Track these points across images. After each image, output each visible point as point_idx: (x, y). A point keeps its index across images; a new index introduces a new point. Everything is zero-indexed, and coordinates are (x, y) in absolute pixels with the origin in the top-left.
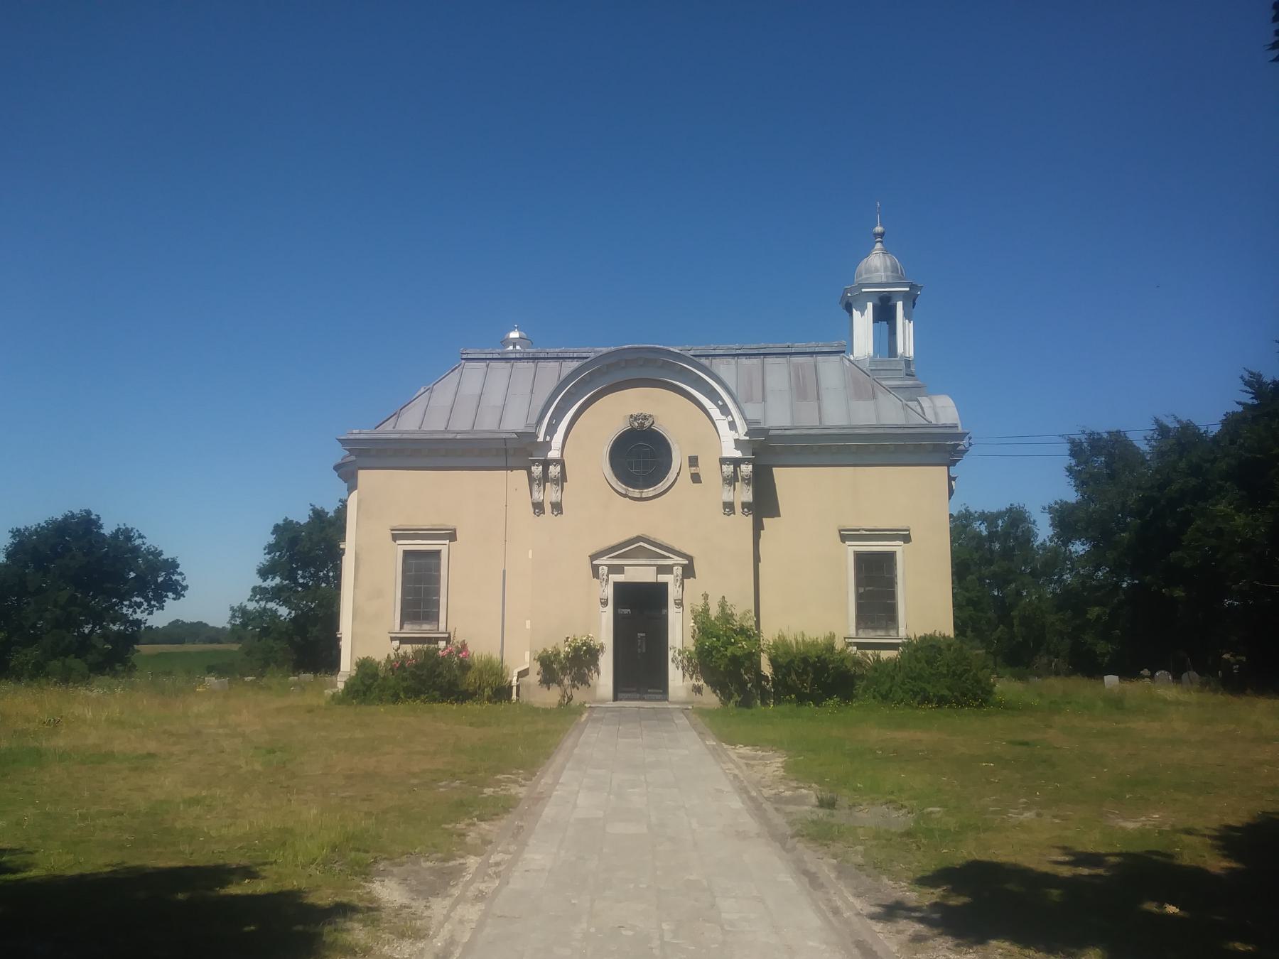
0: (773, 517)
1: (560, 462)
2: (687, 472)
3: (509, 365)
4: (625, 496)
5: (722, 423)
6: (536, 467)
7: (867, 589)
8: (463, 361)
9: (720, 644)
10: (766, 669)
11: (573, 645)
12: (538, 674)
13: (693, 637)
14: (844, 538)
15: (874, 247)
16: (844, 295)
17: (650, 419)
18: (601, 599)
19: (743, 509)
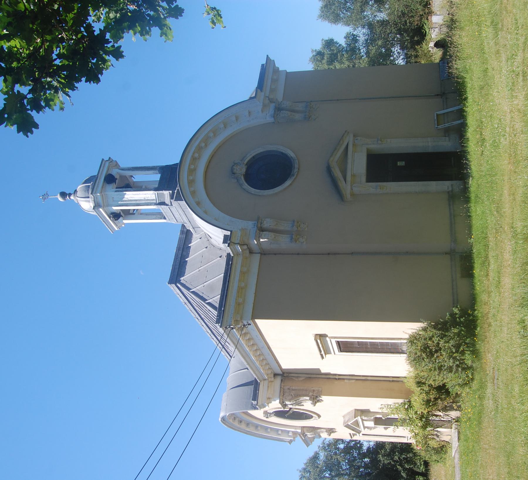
0: (320, 371)
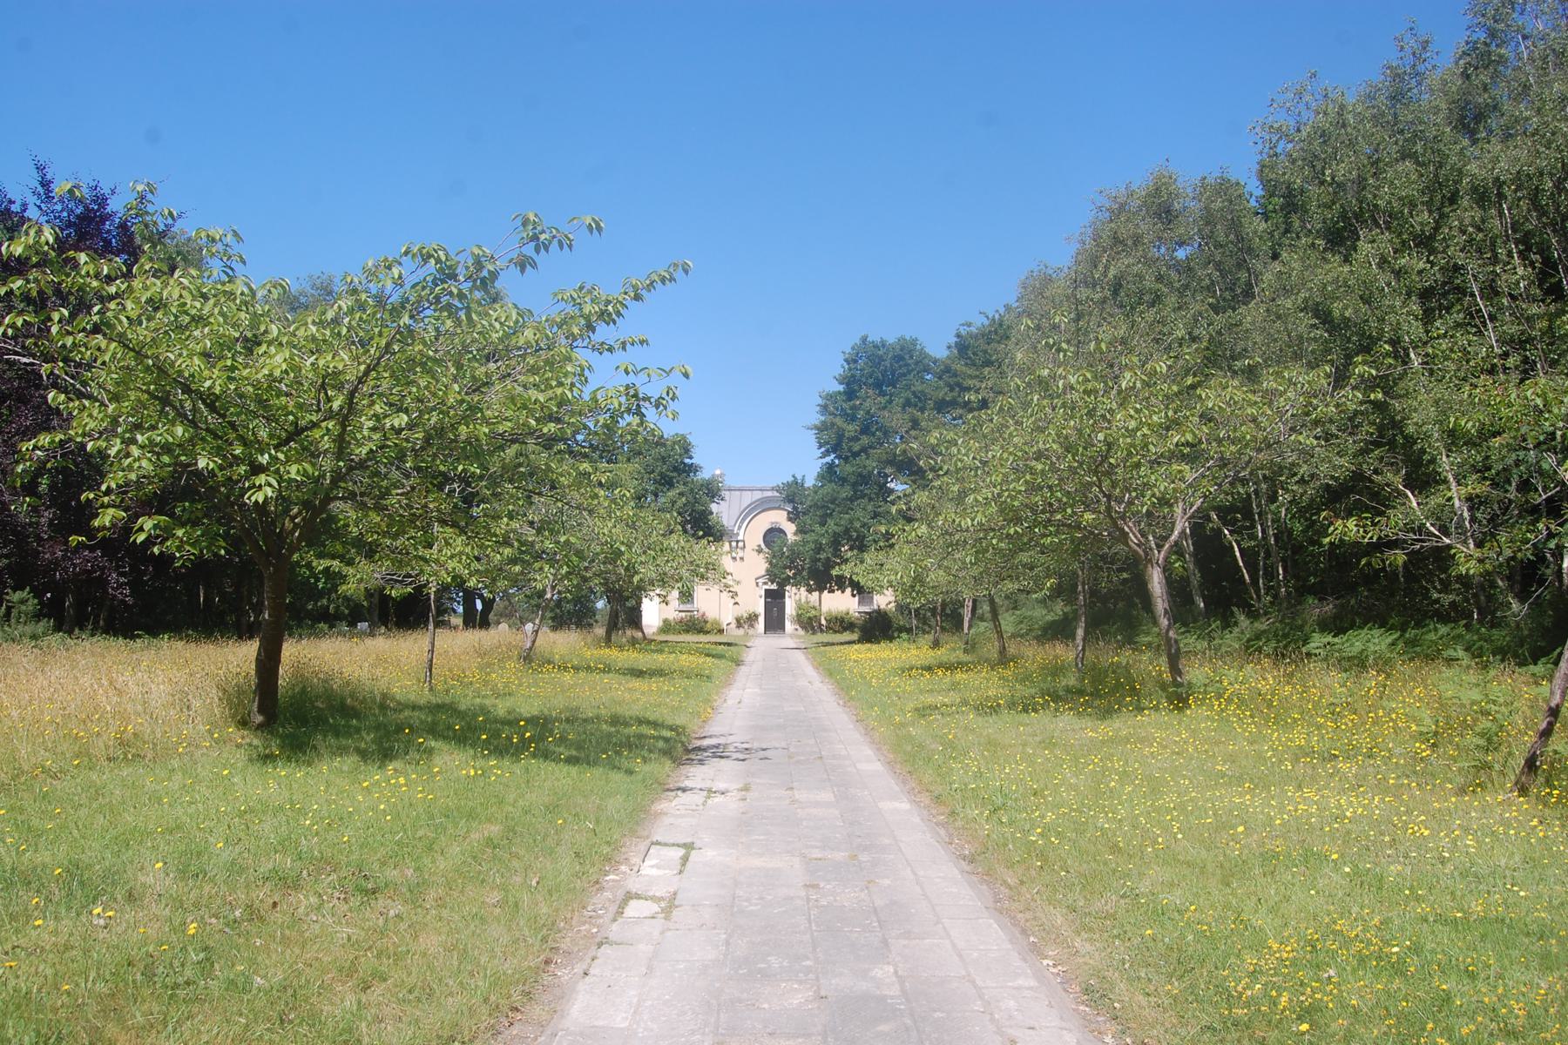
1: (744, 541)
10: (823, 622)
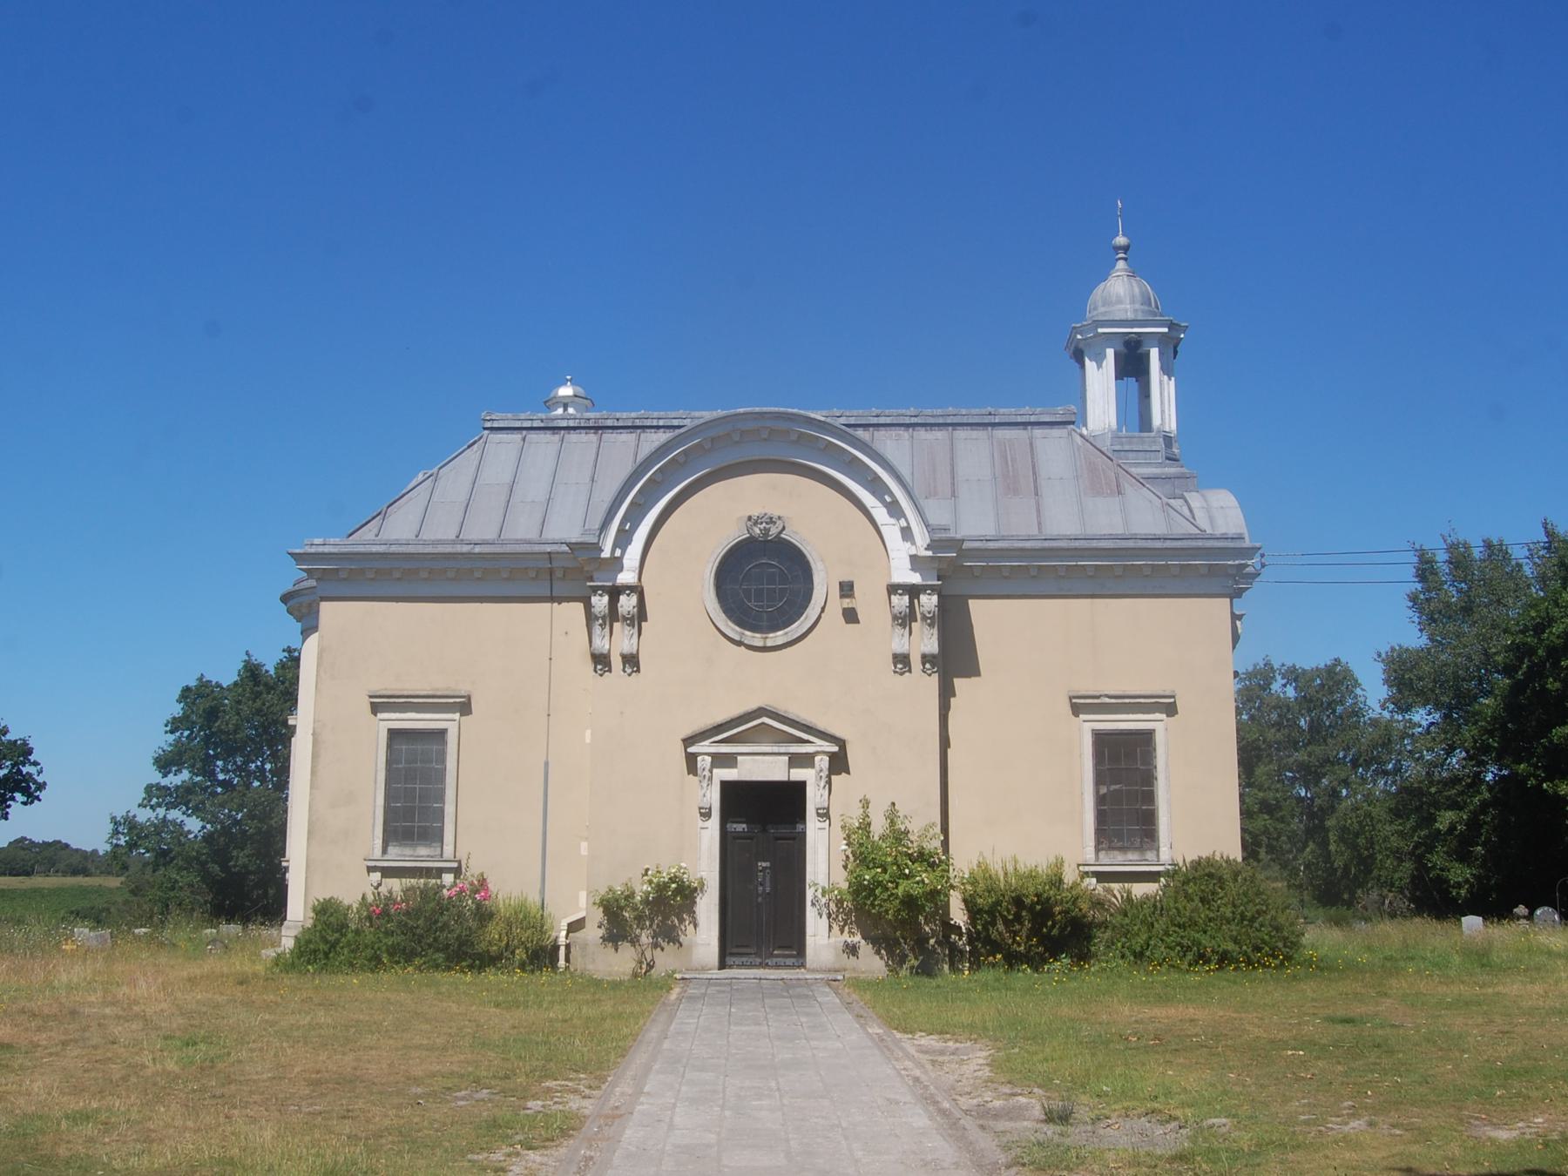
1: (637, 590)
2: (836, 605)
3: (556, 438)
4: (739, 643)
5: (891, 531)
6: (598, 598)
7: (1113, 787)
8: (486, 432)
9: (887, 877)
10: (959, 916)
11: (655, 880)
12: (599, 927)
13: (845, 867)
14: (1077, 709)
15: (1115, 266)
16: (1071, 339)
17: (779, 522)
18: (700, 808)
19: (924, 664)
